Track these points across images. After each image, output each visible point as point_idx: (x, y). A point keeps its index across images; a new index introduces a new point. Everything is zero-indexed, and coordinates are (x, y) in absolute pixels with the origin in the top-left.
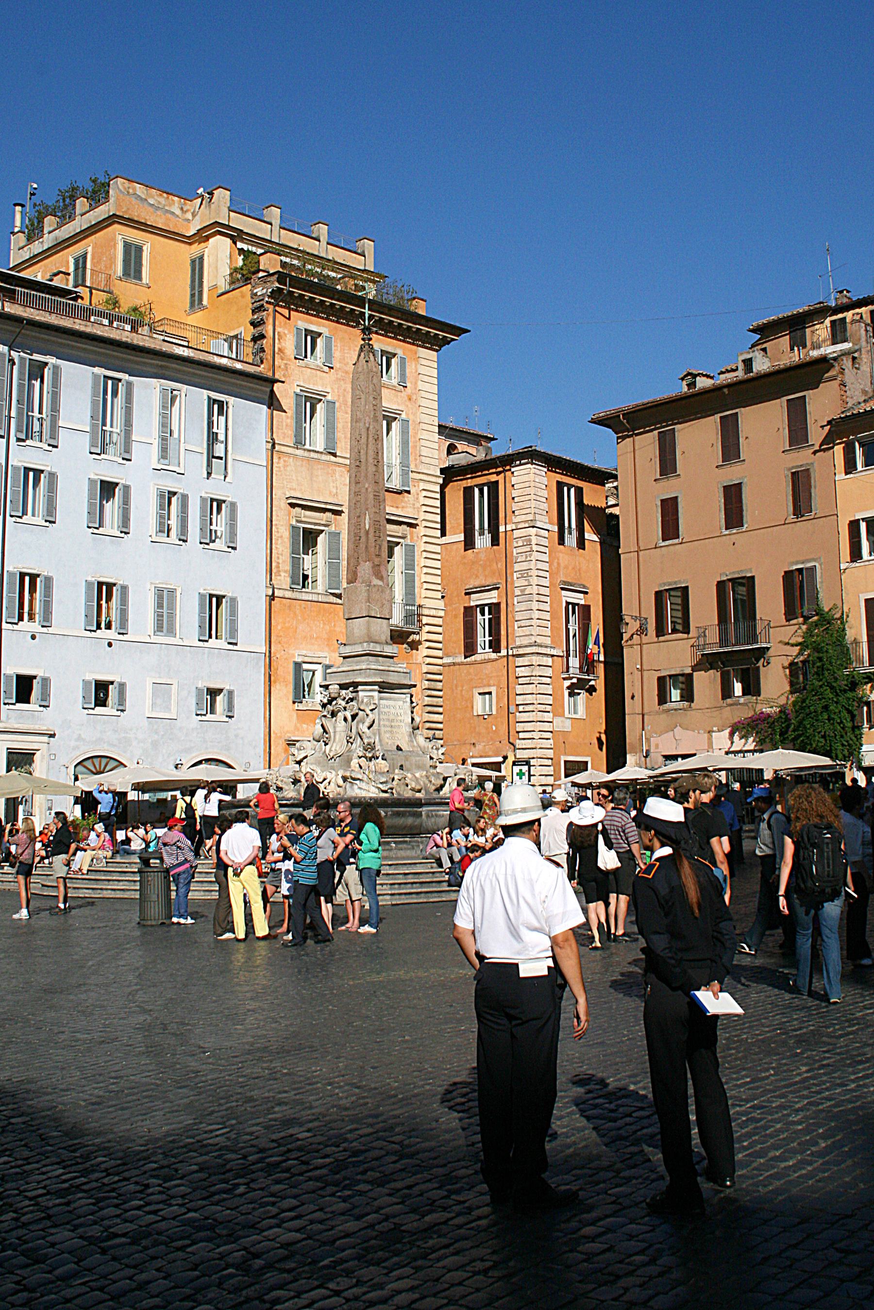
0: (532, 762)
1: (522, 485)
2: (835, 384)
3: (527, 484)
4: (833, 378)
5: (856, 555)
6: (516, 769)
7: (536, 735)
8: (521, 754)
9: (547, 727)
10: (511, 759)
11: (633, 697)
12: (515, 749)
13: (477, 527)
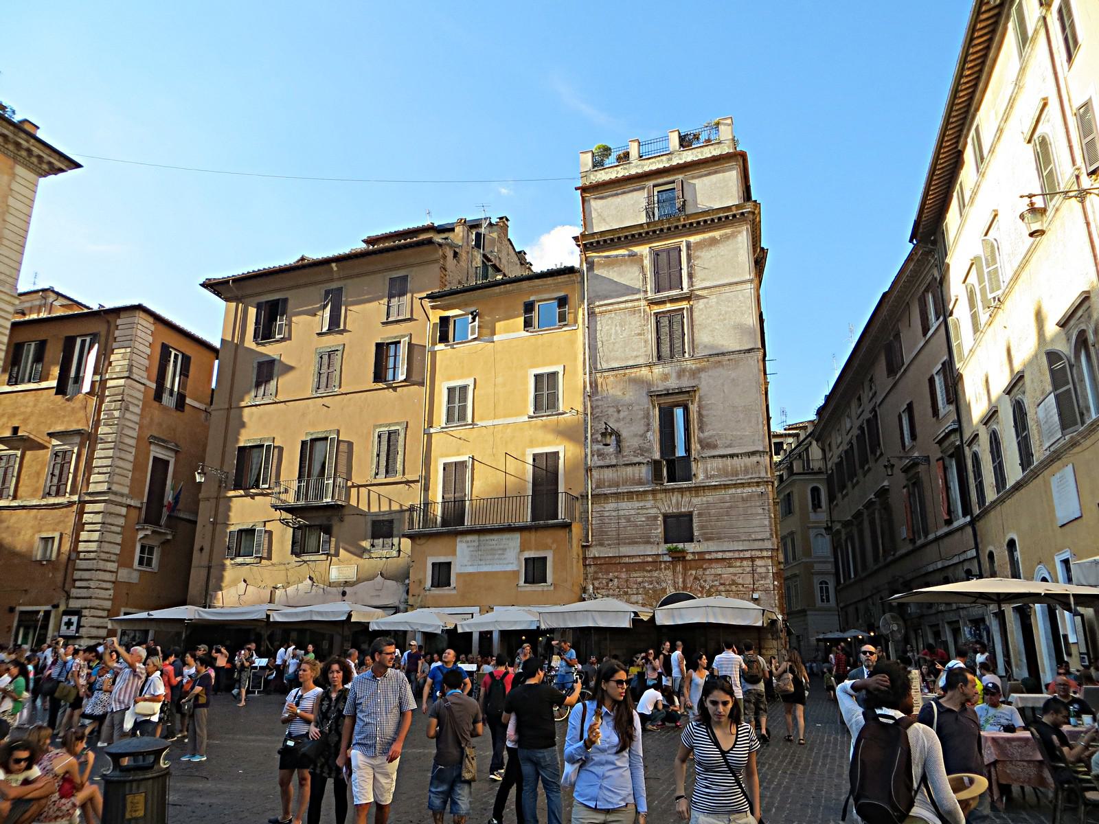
0: (85, 612)
1: (124, 338)
2: (436, 268)
3: (129, 338)
4: (436, 261)
6: (65, 619)
7: (92, 584)
8: (74, 604)
9: (108, 576)
10: (62, 608)
11: (202, 549)
12: (68, 597)
13: (73, 374)
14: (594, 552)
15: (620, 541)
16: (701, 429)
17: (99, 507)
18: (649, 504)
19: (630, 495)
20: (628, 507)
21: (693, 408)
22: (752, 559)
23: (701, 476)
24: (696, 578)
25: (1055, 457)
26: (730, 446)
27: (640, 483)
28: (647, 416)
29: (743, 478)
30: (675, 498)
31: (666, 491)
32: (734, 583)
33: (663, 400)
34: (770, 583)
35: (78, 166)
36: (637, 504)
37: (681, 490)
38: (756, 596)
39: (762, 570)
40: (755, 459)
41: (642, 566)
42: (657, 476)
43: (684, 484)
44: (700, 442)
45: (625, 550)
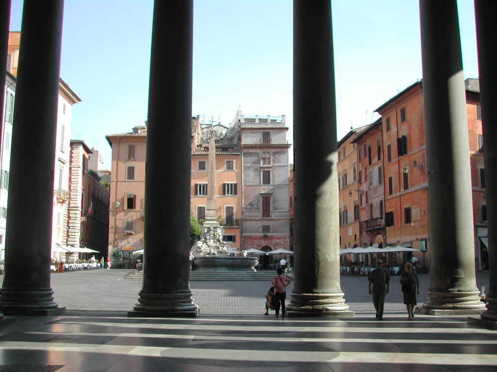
5: (196, 194)
14: (244, 234)
15: (251, 232)
16: (274, 204)
17: (74, 212)
18: (259, 222)
19: (254, 220)
20: (253, 223)
21: (271, 199)
22: (284, 238)
23: (273, 216)
24: (271, 242)
25: (350, 224)
26: (280, 209)
27: (257, 217)
28: (259, 200)
29: (283, 218)
30: (266, 222)
31: (264, 219)
32: (280, 243)
33: (263, 195)
34: (288, 243)
35: (79, 100)
36: (255, 222)
37: (268, 220)
38: (285, 246)
39: (286, 240)
40: (287, 213)
41: (257, 238)
42: (263, 217)
43: (268, 218)
44: (273, 207)
45: (253, 234)
